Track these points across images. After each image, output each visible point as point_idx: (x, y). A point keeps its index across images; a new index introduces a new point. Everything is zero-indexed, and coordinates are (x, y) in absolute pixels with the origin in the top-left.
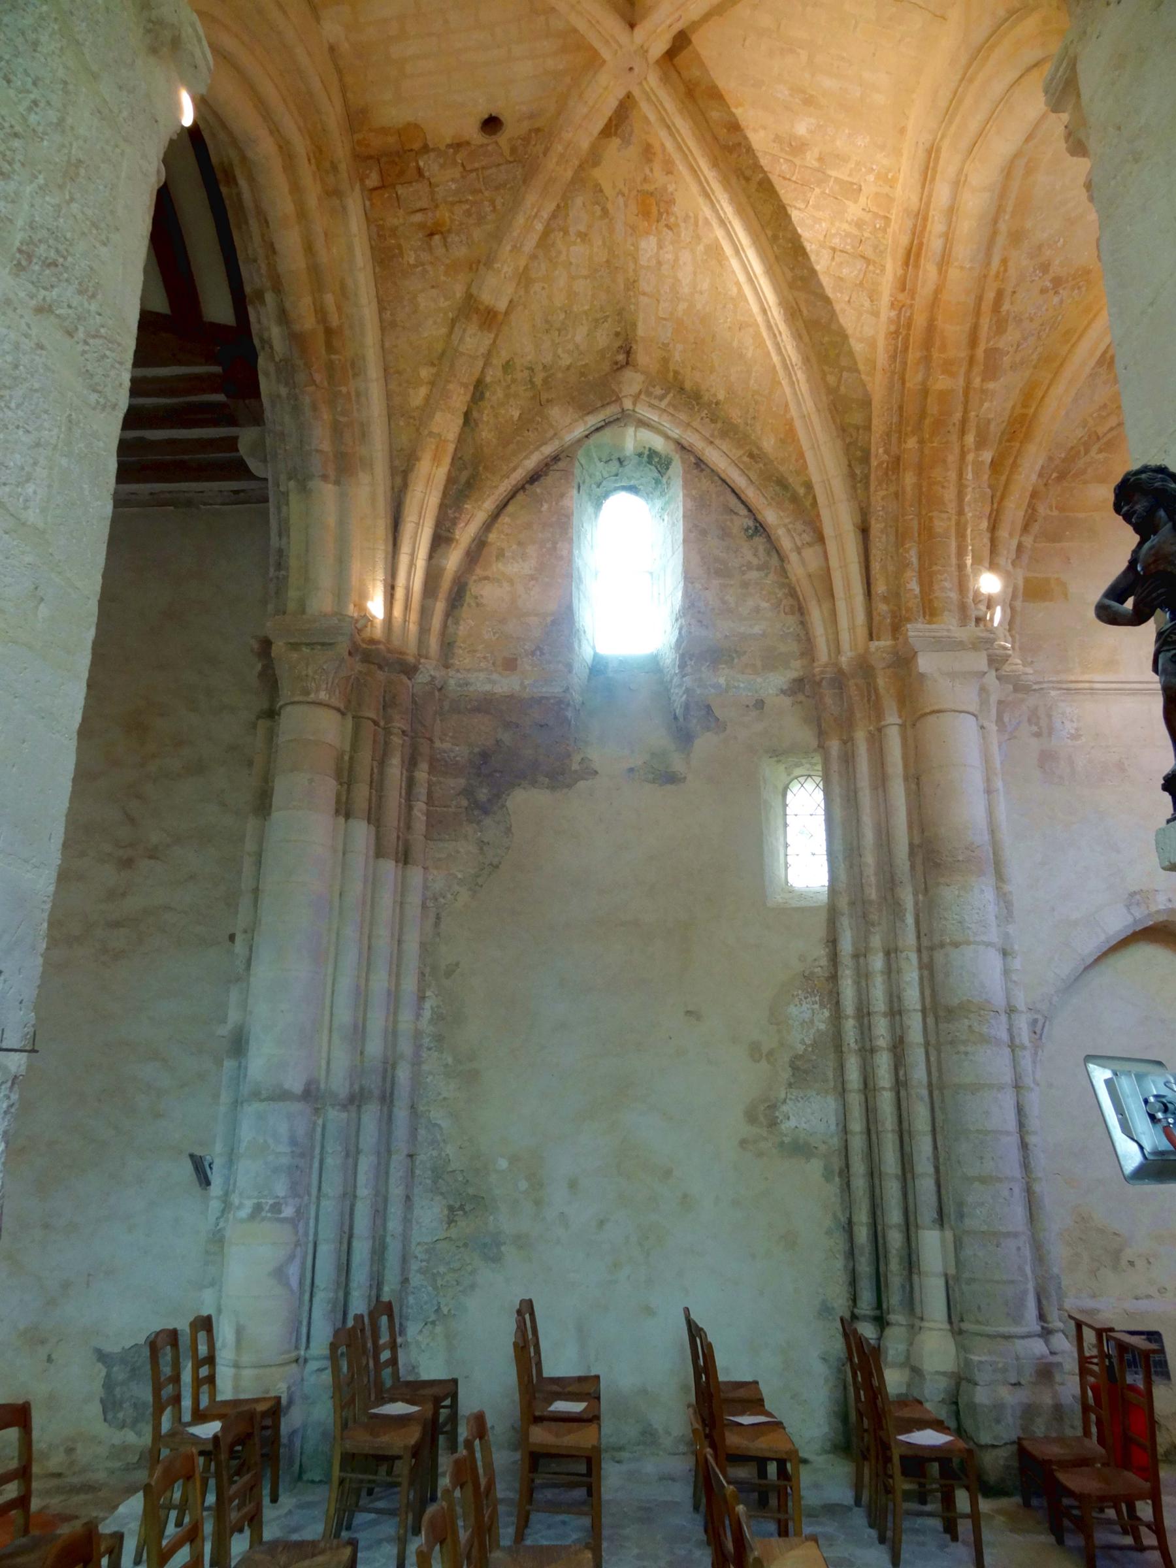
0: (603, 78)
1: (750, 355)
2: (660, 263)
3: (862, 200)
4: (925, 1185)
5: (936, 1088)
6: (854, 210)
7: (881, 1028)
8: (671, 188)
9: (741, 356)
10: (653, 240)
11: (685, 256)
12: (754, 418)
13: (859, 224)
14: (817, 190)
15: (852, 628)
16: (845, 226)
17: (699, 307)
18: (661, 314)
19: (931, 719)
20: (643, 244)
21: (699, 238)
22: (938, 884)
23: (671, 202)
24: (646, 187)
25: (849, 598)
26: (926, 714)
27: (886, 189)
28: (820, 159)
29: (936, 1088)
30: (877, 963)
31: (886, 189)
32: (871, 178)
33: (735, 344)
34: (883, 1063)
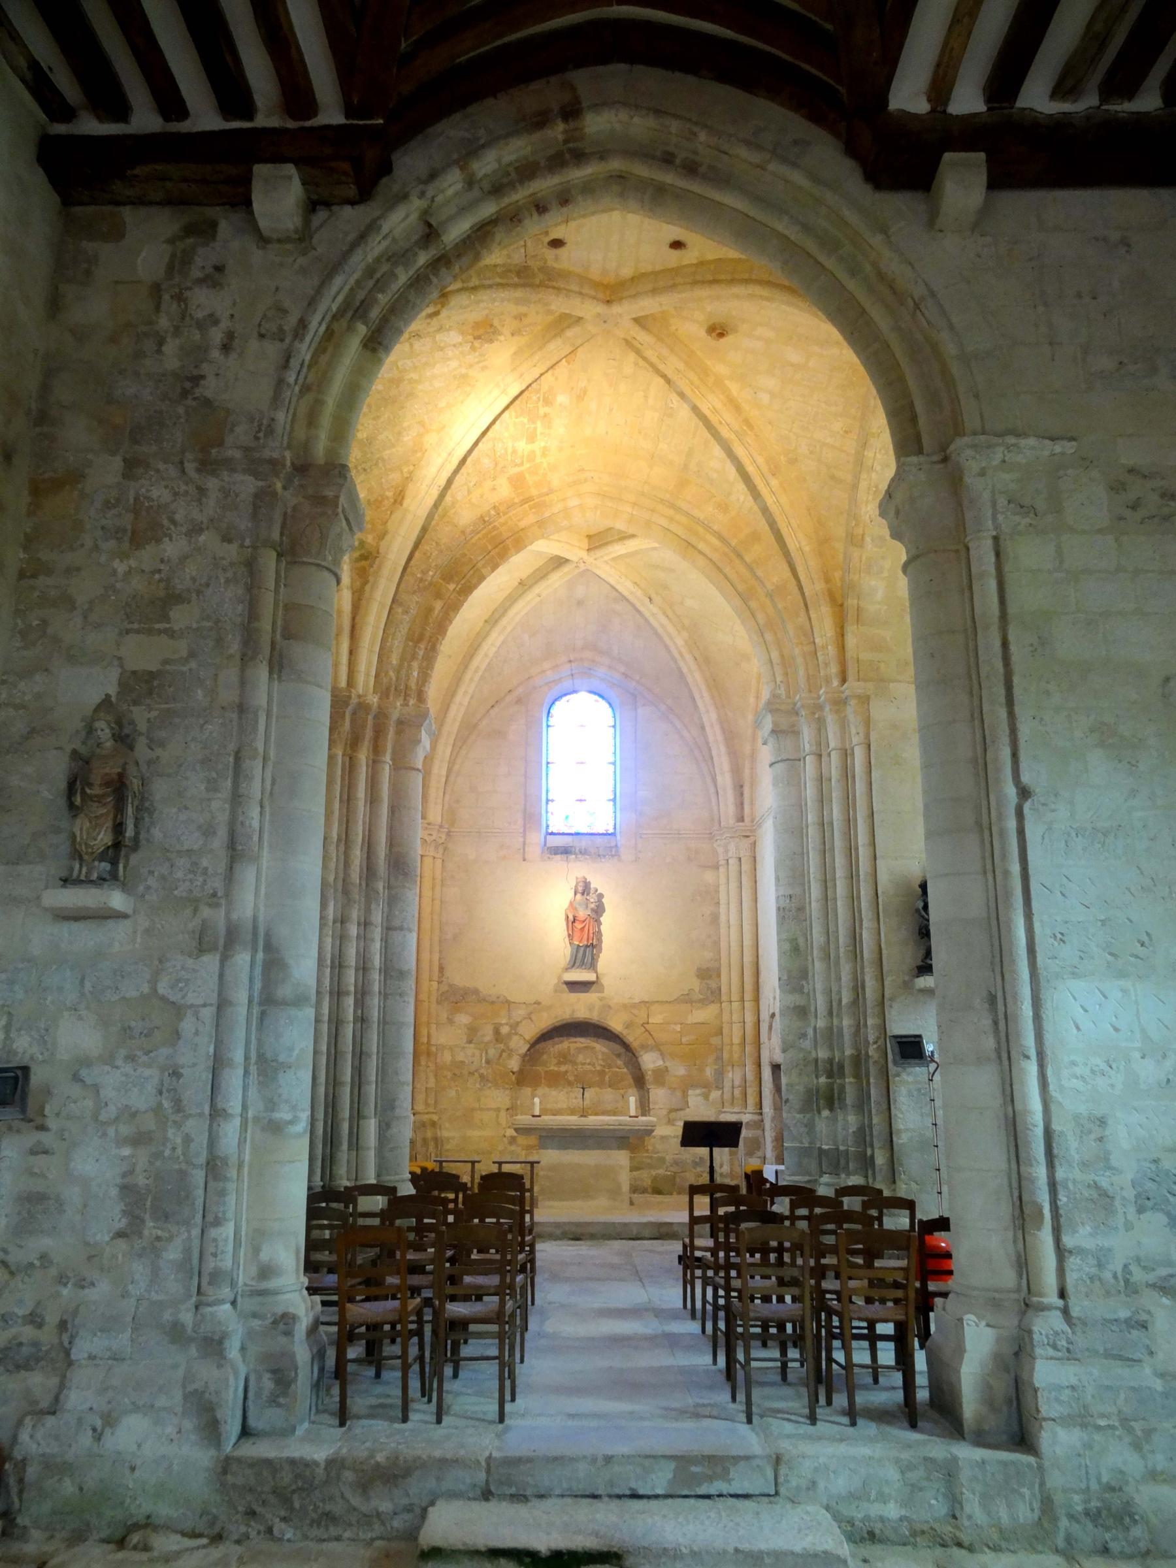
0: (600, 309)
1: (405, 439)
2: (441, 349)
3: (530, 447)
4: (371, 1090)
5: (384, 1022)
6: (522, 446)
7: (350, 977)
8: (502, 338)
9: (399, 433)
10: (459, 339)
11: (454, 364)
12: (365, 470)
13: (514, 452)
14: (525, 420)
15: (367, 675)
16: (510, 445)
17: (420, 387)
18: (400, 364)
19: (414, 772)
20: (452, 333)
21: (471, 366)
22: (404, 887)
23: (491, 341)
24: (496, 322)
25: (371, 651)
26: (414, 769)
27: (538, 454)
28: (545, 415)
29: (384, 1022)
30: (353, 930)
31: (538, 454)
32: (543, 444)
33: (405, 424)
34: (350, 1001)
